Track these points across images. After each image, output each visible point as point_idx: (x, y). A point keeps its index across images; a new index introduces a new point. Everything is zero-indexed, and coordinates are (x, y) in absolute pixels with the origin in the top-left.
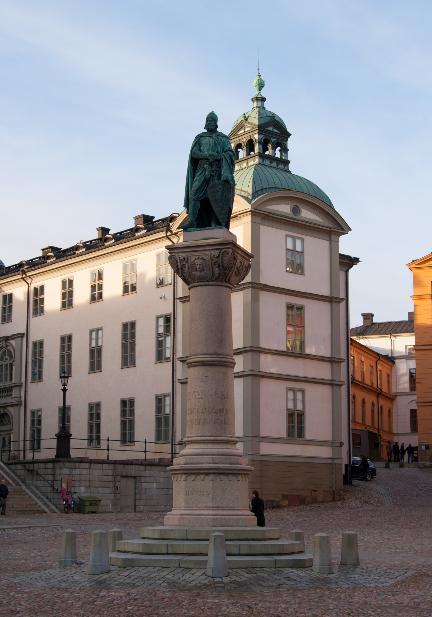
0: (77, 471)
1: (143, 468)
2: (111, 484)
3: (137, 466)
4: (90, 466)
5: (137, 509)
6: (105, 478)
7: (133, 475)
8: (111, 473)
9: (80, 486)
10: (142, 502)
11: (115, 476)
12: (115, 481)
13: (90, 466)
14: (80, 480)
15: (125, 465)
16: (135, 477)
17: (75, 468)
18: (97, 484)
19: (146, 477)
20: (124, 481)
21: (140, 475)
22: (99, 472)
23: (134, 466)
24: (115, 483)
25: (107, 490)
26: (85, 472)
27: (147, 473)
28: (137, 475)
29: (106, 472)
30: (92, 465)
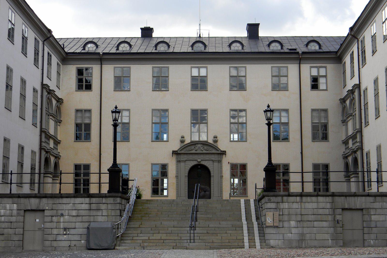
0: (286, 205)
1: (371, 199)
2: (330, 218)
3: (364, 198)
4: (302, 199)
5: (366, 244)
6: (321, 211)
7: (358, 207)
8: (328, 206)
9: (289, 221)
10: (373, 236)
11: (334, 209)
12: (334, 215)
13: (302, 199)
14: (289, 215)
15: (347, 197)
16: (362, 209)
17: (282, 202)
18: (311, 218)
19: (376, 209)
20: (348, 214)
21: (367, 207)
22: (315, 205)
23: (359, 198)
24: (334, 217)
25: (325, 224)
26: (295, 206)
27: (377, 205)
28: (363, 207)
29: (321, 205)
30: (304, 199)
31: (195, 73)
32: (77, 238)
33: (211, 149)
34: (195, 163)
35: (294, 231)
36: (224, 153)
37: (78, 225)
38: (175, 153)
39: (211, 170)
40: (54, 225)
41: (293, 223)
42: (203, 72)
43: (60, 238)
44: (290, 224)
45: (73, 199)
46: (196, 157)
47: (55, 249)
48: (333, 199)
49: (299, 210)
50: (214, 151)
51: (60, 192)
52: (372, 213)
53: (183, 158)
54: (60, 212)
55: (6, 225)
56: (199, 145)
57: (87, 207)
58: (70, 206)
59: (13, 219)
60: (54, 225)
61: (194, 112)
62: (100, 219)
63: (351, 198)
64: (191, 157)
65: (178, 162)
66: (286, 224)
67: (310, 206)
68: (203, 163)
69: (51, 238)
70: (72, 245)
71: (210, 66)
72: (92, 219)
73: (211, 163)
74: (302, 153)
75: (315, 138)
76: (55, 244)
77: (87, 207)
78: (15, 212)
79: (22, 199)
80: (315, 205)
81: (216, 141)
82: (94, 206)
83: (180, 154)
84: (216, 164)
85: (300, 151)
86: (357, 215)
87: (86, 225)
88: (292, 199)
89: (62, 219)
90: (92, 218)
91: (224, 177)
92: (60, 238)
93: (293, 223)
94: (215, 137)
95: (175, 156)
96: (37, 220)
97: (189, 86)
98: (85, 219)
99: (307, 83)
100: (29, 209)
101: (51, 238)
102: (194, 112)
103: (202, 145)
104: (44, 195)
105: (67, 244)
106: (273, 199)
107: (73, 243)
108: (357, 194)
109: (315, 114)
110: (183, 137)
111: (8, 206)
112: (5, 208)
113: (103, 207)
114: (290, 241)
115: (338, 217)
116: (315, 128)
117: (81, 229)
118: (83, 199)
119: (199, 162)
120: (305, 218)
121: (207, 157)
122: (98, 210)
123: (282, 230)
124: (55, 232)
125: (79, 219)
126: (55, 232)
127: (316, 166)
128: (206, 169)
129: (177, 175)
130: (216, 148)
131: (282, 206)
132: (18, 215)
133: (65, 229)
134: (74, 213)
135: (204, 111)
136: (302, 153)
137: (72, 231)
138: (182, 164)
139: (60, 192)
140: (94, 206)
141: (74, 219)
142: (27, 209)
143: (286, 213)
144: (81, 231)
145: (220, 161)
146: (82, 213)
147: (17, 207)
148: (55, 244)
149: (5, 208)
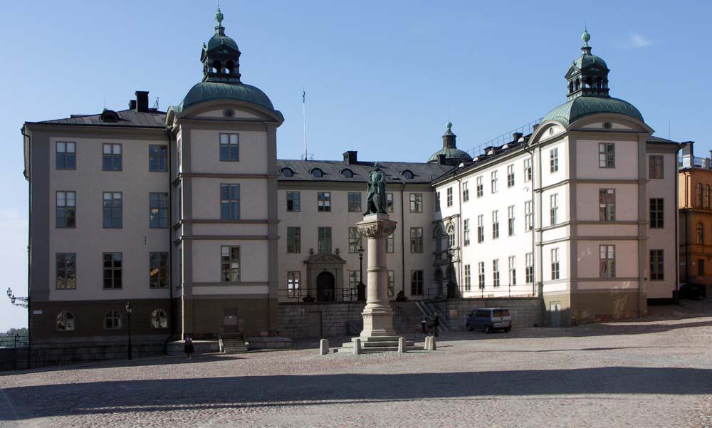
0: (460, 306)
26: (466, 306)
32: (342, 328)
34: (322, 271)
36: (345, 262)
38: (305, 262)
54: (331, 313)
57: (346, 309)
58: (337, 310)
59: (303, 318)
61: (321, 229)
65: (309, 270)
77: (346, 309)
78: (304, 314)
82: (351, 309)
87: (346, 320)
89: (332, 318)
94: (337, 250)
95: (306, 265)
102: (321, 229)
106: (453, 302)
107: (339, 332)
110: (312, 250)
111: (299, 310)
124: (329, 325)
128: (330, 275)
130: (340, 259)
134: (339, 313)
135: (329, 229)
140: (351, 309)
145: (342, 269)
148: (329, 333)
149: (297, 311)
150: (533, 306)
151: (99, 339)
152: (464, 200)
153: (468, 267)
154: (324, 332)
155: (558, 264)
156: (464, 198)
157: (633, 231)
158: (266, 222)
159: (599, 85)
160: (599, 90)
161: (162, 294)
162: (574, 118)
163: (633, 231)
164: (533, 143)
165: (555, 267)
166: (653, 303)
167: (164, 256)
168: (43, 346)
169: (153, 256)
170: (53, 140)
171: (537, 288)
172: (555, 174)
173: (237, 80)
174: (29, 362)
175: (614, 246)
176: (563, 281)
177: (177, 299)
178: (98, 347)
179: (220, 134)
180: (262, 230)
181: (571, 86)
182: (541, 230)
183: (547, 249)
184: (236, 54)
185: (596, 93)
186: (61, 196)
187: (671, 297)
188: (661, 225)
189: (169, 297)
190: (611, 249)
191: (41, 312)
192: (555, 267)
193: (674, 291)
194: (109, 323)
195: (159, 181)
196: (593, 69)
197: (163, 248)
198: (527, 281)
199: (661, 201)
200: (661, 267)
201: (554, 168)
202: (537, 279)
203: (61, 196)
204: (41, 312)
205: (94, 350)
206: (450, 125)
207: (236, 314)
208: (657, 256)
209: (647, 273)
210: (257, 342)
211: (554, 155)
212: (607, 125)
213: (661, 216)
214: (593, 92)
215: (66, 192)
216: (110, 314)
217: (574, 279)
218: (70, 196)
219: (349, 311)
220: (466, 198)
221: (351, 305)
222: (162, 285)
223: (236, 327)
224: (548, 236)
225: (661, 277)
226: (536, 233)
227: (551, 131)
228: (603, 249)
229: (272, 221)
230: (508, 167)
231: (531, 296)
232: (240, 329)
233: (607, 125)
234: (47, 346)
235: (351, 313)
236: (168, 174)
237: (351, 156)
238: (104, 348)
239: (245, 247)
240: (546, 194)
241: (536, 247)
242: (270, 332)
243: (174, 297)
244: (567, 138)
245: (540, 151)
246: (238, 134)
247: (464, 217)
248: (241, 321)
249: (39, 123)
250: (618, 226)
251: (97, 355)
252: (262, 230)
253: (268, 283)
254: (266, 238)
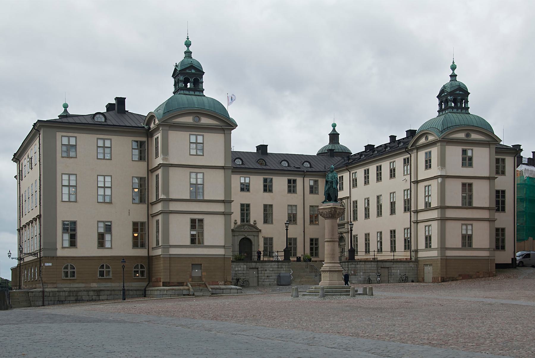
0: (359, 266)
1: (392, 263)
2: (376, 271)
3: (389, 263)
4: (365, 263)
5: (390, 282)
6: (372, 268)
7: (387, 267)
8: (375, 266)
9: (360, 272)
10: (392, 279)
11: (377, 267)
12: (378, 270)
13: (365, 263)
14: (360, 270)
15: (383, 263)
16: (388, 268)
17: (357, 264)
18: (369, 271)
19: (394, 267)
20: (383, 269)
21: (390, 266)
22: (370, 266)
23: (387, 263)
24: (378, 271)
25: (374, 274)
26: (363, 266)
27: (394, 266)
28: (389, 267)
29: (373, 266)
30: (366, 263)
31: (242, 181)
32: (273, 280)
33: (253, 228)
34: (243, 237)
35: (362, 277)
36: (260, 231)
37: (273, 275)
39: (253, 241)
40: (263, 275)
41: (361, 273)
42: (247, 180)
43: (266, 280)
44: (360, 274)
45: (270, 263)
46: (244, 233)
47: (264, 285)
48: (377, 263)
49: (364, 268)
50: (255, 230)
51: (263, 260)
52: (392, 269)
53: (237, 234)
54: (265, 269)
55: (241, 275)
56: (246, 226)
57: (277, 266)
58: (269, 266)
59: (245, 272)
60: (263, 275)
62: (282, 272)
63: (384, 263)
64: (241, 233)
66: (359, 274)
67: (368, 266)
68: (248, 237)
69: (261, 280)
70: (271, 284)
71: (251, 176)
72: (279, 272)
73: (253, 237)
74: (304, 232)
75: (311, 222)
76: (263, 283)
77: (277, 266)
78: (245, 269)
79: (248, 263)
80: (370, 266)
81: (255, 224)
82: (280, 266)
83: (235, 231)
84: (256, 238)
85: (303, 230)
86: (386, 270)
87: (277, 275)
88: (361, 263)
89: (266, 272)
90: (279, 271)
91: (260, 246)
92: (266, 280)
93: (361, 273)
94: (255, 221)
96: (254, 273)
97: (239, 189)
98: (276, 272)
99: (307, 189)
100: (251, 267)
101: (261, 280)
103: (248, 226)
104: (254, 261)
105: (269, 283)
106: (354, 263)
108: (387, 261)
109: (311, 207)
111: (242, 266)
112: (241, 267)
113: (284, 266)
114: (360, 281)
115: (379, 271)
116: (311, 217)
117: (274, 277)
118: (275, 263)
119: (246, 236)
120: (366, 271)
121: (251, 233)
122: (282, 268)
123: (357, 276)
124: (263, 278)
125: (274, 272)
126: (263, 278)
127: (312, 240)
128: (249, 240)
129: (233, 244)
130: (257, 228)
131: (357, 266)
132: (247, 270)
133: (268, 277)
134: (271, 269)
135: (248, 206)
136: (304, 232)
137: (271, 278)
138: (236, 237)
139: (263, 260)
140: (280, 266)
141: (271, 272)
142: (250, 267)
143: (359, 269)
144: (274, 277)
145: (258, 236)
146: (275, 269)
147: (246, 266)
148: (263, 283)
149: (241, 267)
150: (411, 267)
151: (94, 285)
152: (353, 187)
153: (356, 237)
154: (260, 283)
155: (430, 237)
156: (353, 185)
157: (485, 214)
158: (223, 201)
159: (461, 104)
160: (462, 108)
161: (141, 252)
162: (444, 129)
163: (485, 214)
164: (411, 147)
165: (428, 239)
166: (501, 267)
167: (142, 224)
168: (53, 290)
169: (135, 224)
170: (59, 135)
171: (413, 254)
172: (429, 171)
173: (201, 94)
174: (43, 301)
175: (472, 225)
176: (434, 249)
177: (152, 256)
178: (94, 291)
179: (190, 135)
180: (220, 208)
181: (440, 105)
182: (417, 212)
183: (421, 226)
184: (201, 73)
185: (460, 111)
186: (65, 177)
187: (511, 262)
188: (503, 210)
189: (147, 255)
190: (469, 227)
191: (50, 264)
192: (428, 239)
193: (512, 259)
194: (102, 274)
195: (141, 169)
196: (458, 92)
197: (142, 218)
198: (405, 249)
199: (503, 192)
200: (503, 241)
201: (428, 165)
202: (413, 248)
203: (65, 177)
204: (50, 264)
205: (91, 293)
206: (334, 126)
207: (201, 269)
208: (499, 233)
209: (494, 247)
210: (217, 289)
211: (428, 155)
212: (468, 135)
213: (503, 202)
214: (457, 110)
215: (69, 175)
216: (66, 268)
217: (443, 248)
218: (73, 178)
219: (278, 268)
220: (355, 185)
221: (280, 263)
222: (143, 246)
223: (200, 278)
224: (422, 216)
225: (503, 248)
226: (412, 213)
227: (427, 138)
228: (464, 227)
229: (227, 202)
230: (390, 163)
231: (409, 260)
232: (204, 279)
233: (468, 135)
234: (56, 290)
235: (279, 269)
236: (146, 163)
237: (262, 149)
238: (98, 292)
239: (207, 220)
240: (421, 186)
241: (412, 224)
242: (225, 282)
243: (151, 254)
244: (439, 144)
245: (417, 152)
246: (203, 136)
247: (353, 199)
248: (204, 274)
249: (47, 121)
250: (475, 211)
251: (94, 297)
252: (220, 208)
253: (224, 247)
254: (223, 214)
